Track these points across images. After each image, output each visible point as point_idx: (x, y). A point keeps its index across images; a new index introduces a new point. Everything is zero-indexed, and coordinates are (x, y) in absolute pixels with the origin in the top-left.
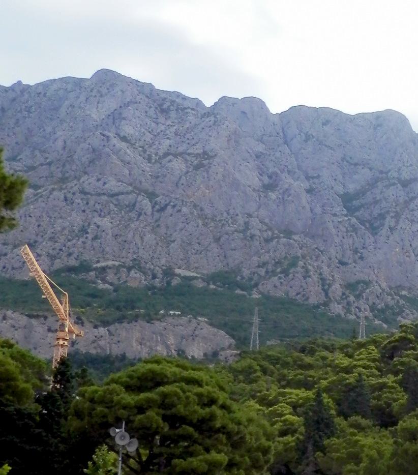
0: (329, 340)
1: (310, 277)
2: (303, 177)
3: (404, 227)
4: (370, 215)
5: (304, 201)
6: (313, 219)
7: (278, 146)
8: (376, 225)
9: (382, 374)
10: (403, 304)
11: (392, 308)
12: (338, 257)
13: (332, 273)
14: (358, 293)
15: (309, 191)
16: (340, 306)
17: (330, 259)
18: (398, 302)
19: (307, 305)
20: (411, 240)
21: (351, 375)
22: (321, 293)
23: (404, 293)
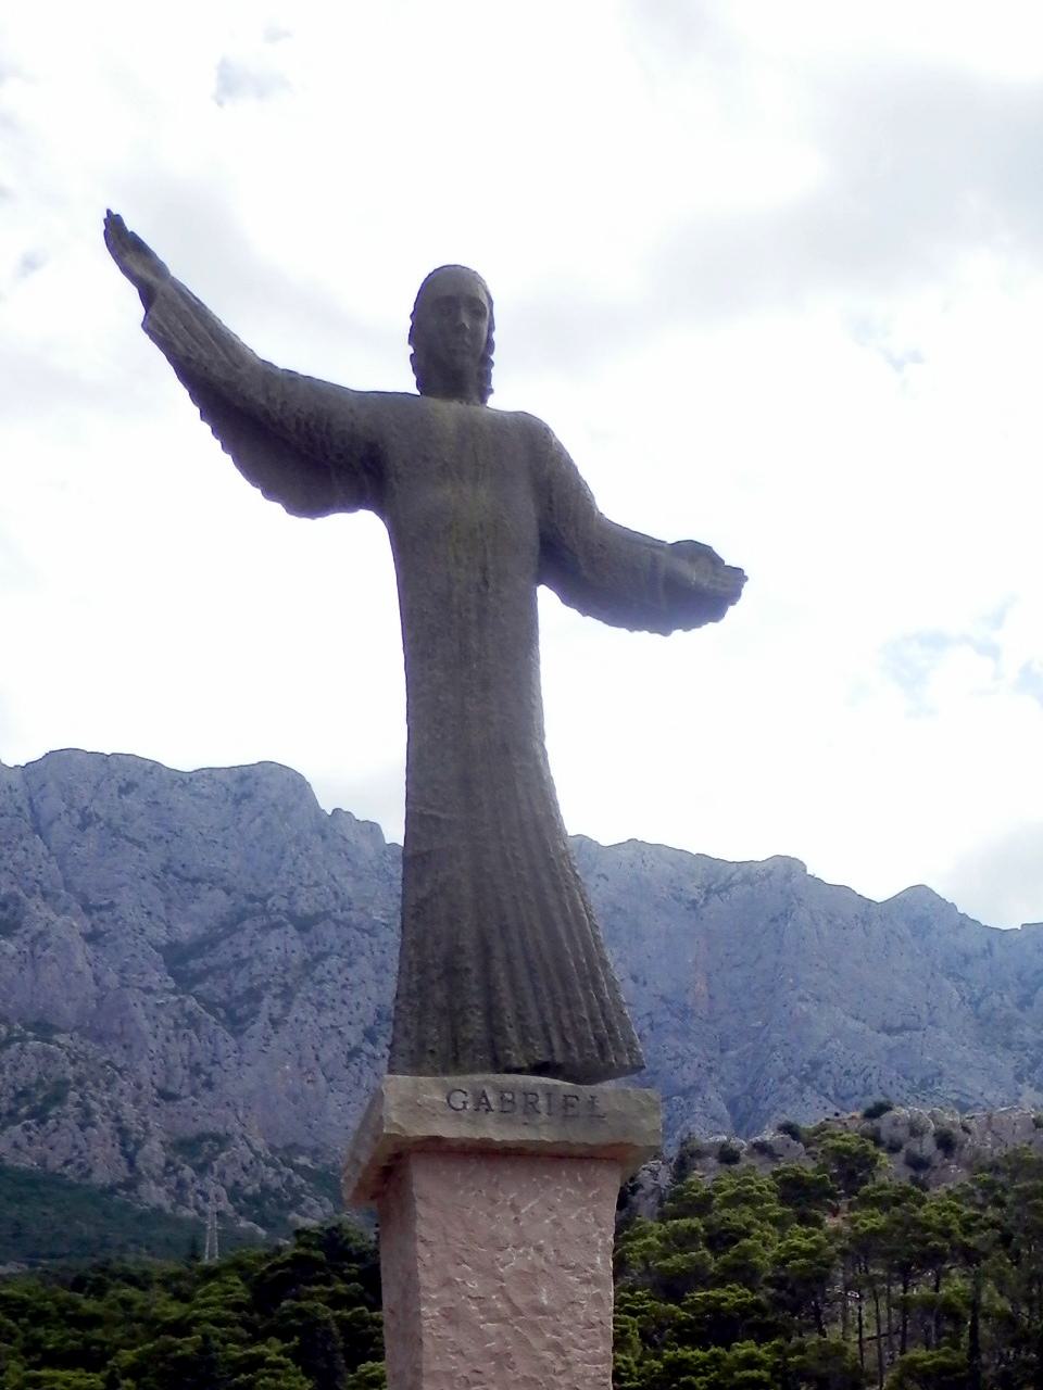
0: (137, 1262)
1: (93, 1125)
2: (76, 906)
3: (302, 1017)
4: (229, 993)
5: (80, 962)
6: (100, 1000)
7: (21, 838)
8: (240, 1012)
9: (259, 1336)
10: (302, 1186)
11: (277, 1194)
12: (156, 1081)
13: (143, 1118)
14: (200, 1161)
15: (92, 937)
16: (161, 1190)
17: (139, 1086)
18: (290, 1179)
19: (88, 1186)
20: (317, 1045)
21: (188, 1339)
22: (118, 1161)
23: (302, 1160)
